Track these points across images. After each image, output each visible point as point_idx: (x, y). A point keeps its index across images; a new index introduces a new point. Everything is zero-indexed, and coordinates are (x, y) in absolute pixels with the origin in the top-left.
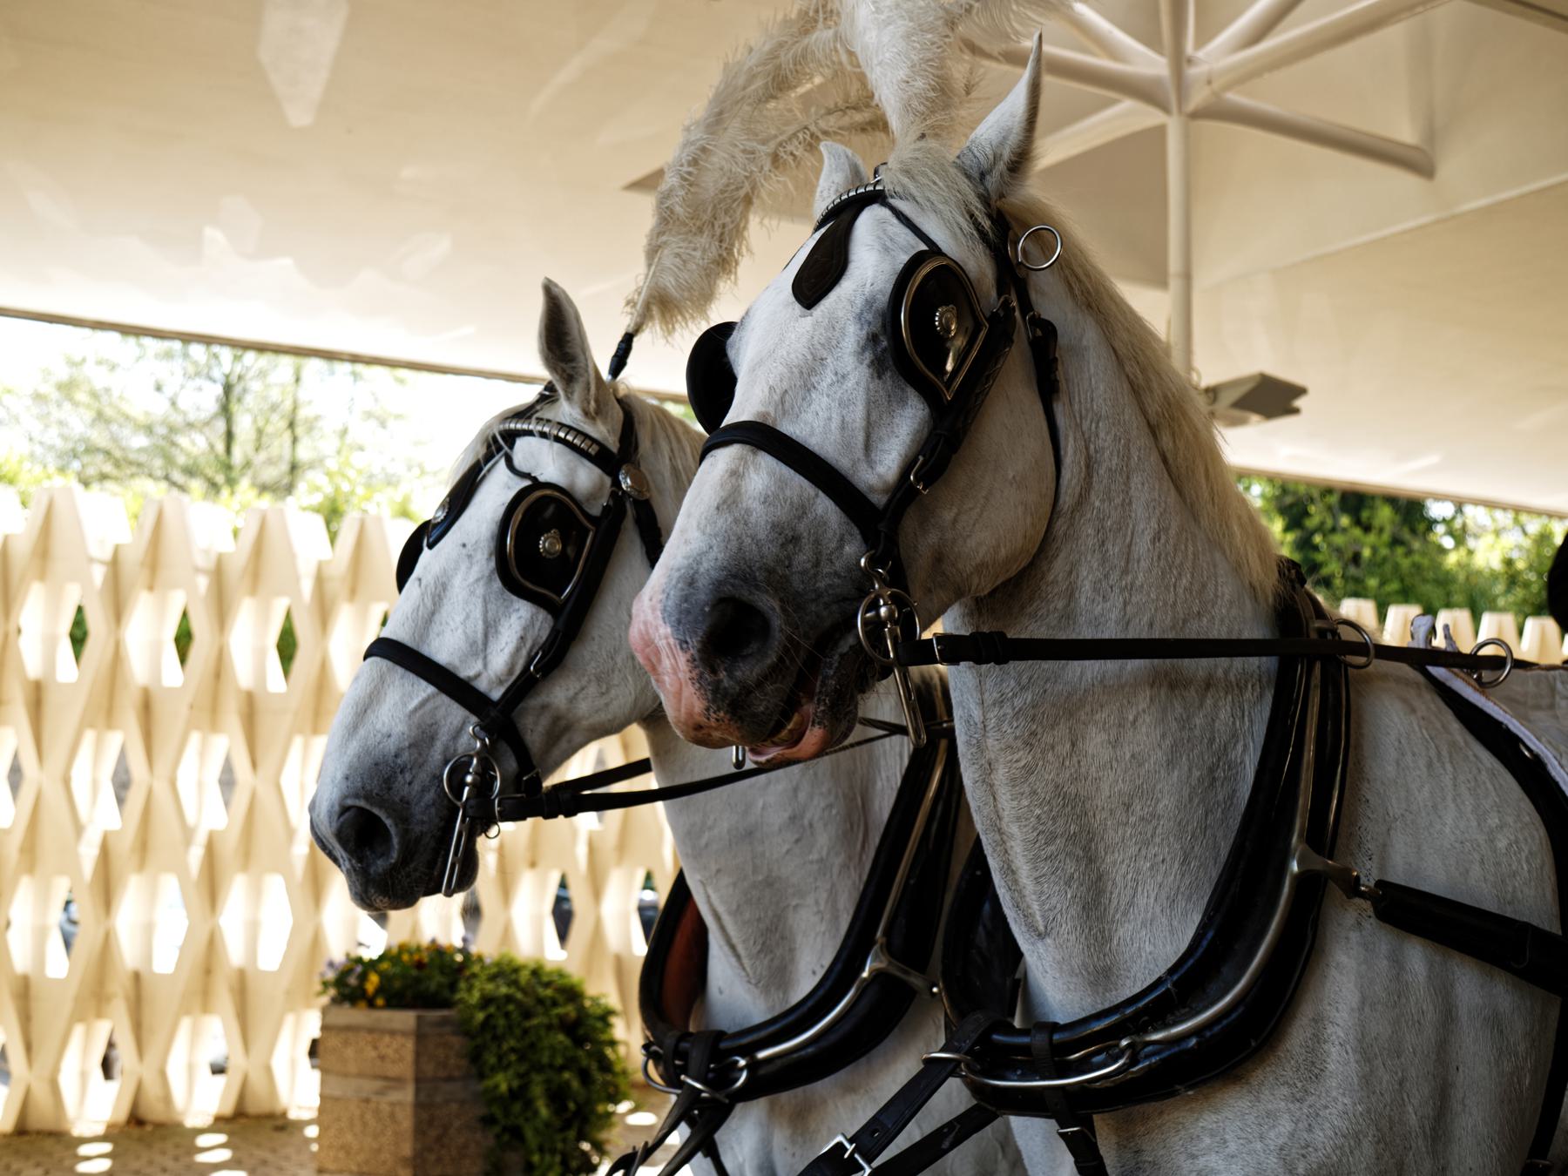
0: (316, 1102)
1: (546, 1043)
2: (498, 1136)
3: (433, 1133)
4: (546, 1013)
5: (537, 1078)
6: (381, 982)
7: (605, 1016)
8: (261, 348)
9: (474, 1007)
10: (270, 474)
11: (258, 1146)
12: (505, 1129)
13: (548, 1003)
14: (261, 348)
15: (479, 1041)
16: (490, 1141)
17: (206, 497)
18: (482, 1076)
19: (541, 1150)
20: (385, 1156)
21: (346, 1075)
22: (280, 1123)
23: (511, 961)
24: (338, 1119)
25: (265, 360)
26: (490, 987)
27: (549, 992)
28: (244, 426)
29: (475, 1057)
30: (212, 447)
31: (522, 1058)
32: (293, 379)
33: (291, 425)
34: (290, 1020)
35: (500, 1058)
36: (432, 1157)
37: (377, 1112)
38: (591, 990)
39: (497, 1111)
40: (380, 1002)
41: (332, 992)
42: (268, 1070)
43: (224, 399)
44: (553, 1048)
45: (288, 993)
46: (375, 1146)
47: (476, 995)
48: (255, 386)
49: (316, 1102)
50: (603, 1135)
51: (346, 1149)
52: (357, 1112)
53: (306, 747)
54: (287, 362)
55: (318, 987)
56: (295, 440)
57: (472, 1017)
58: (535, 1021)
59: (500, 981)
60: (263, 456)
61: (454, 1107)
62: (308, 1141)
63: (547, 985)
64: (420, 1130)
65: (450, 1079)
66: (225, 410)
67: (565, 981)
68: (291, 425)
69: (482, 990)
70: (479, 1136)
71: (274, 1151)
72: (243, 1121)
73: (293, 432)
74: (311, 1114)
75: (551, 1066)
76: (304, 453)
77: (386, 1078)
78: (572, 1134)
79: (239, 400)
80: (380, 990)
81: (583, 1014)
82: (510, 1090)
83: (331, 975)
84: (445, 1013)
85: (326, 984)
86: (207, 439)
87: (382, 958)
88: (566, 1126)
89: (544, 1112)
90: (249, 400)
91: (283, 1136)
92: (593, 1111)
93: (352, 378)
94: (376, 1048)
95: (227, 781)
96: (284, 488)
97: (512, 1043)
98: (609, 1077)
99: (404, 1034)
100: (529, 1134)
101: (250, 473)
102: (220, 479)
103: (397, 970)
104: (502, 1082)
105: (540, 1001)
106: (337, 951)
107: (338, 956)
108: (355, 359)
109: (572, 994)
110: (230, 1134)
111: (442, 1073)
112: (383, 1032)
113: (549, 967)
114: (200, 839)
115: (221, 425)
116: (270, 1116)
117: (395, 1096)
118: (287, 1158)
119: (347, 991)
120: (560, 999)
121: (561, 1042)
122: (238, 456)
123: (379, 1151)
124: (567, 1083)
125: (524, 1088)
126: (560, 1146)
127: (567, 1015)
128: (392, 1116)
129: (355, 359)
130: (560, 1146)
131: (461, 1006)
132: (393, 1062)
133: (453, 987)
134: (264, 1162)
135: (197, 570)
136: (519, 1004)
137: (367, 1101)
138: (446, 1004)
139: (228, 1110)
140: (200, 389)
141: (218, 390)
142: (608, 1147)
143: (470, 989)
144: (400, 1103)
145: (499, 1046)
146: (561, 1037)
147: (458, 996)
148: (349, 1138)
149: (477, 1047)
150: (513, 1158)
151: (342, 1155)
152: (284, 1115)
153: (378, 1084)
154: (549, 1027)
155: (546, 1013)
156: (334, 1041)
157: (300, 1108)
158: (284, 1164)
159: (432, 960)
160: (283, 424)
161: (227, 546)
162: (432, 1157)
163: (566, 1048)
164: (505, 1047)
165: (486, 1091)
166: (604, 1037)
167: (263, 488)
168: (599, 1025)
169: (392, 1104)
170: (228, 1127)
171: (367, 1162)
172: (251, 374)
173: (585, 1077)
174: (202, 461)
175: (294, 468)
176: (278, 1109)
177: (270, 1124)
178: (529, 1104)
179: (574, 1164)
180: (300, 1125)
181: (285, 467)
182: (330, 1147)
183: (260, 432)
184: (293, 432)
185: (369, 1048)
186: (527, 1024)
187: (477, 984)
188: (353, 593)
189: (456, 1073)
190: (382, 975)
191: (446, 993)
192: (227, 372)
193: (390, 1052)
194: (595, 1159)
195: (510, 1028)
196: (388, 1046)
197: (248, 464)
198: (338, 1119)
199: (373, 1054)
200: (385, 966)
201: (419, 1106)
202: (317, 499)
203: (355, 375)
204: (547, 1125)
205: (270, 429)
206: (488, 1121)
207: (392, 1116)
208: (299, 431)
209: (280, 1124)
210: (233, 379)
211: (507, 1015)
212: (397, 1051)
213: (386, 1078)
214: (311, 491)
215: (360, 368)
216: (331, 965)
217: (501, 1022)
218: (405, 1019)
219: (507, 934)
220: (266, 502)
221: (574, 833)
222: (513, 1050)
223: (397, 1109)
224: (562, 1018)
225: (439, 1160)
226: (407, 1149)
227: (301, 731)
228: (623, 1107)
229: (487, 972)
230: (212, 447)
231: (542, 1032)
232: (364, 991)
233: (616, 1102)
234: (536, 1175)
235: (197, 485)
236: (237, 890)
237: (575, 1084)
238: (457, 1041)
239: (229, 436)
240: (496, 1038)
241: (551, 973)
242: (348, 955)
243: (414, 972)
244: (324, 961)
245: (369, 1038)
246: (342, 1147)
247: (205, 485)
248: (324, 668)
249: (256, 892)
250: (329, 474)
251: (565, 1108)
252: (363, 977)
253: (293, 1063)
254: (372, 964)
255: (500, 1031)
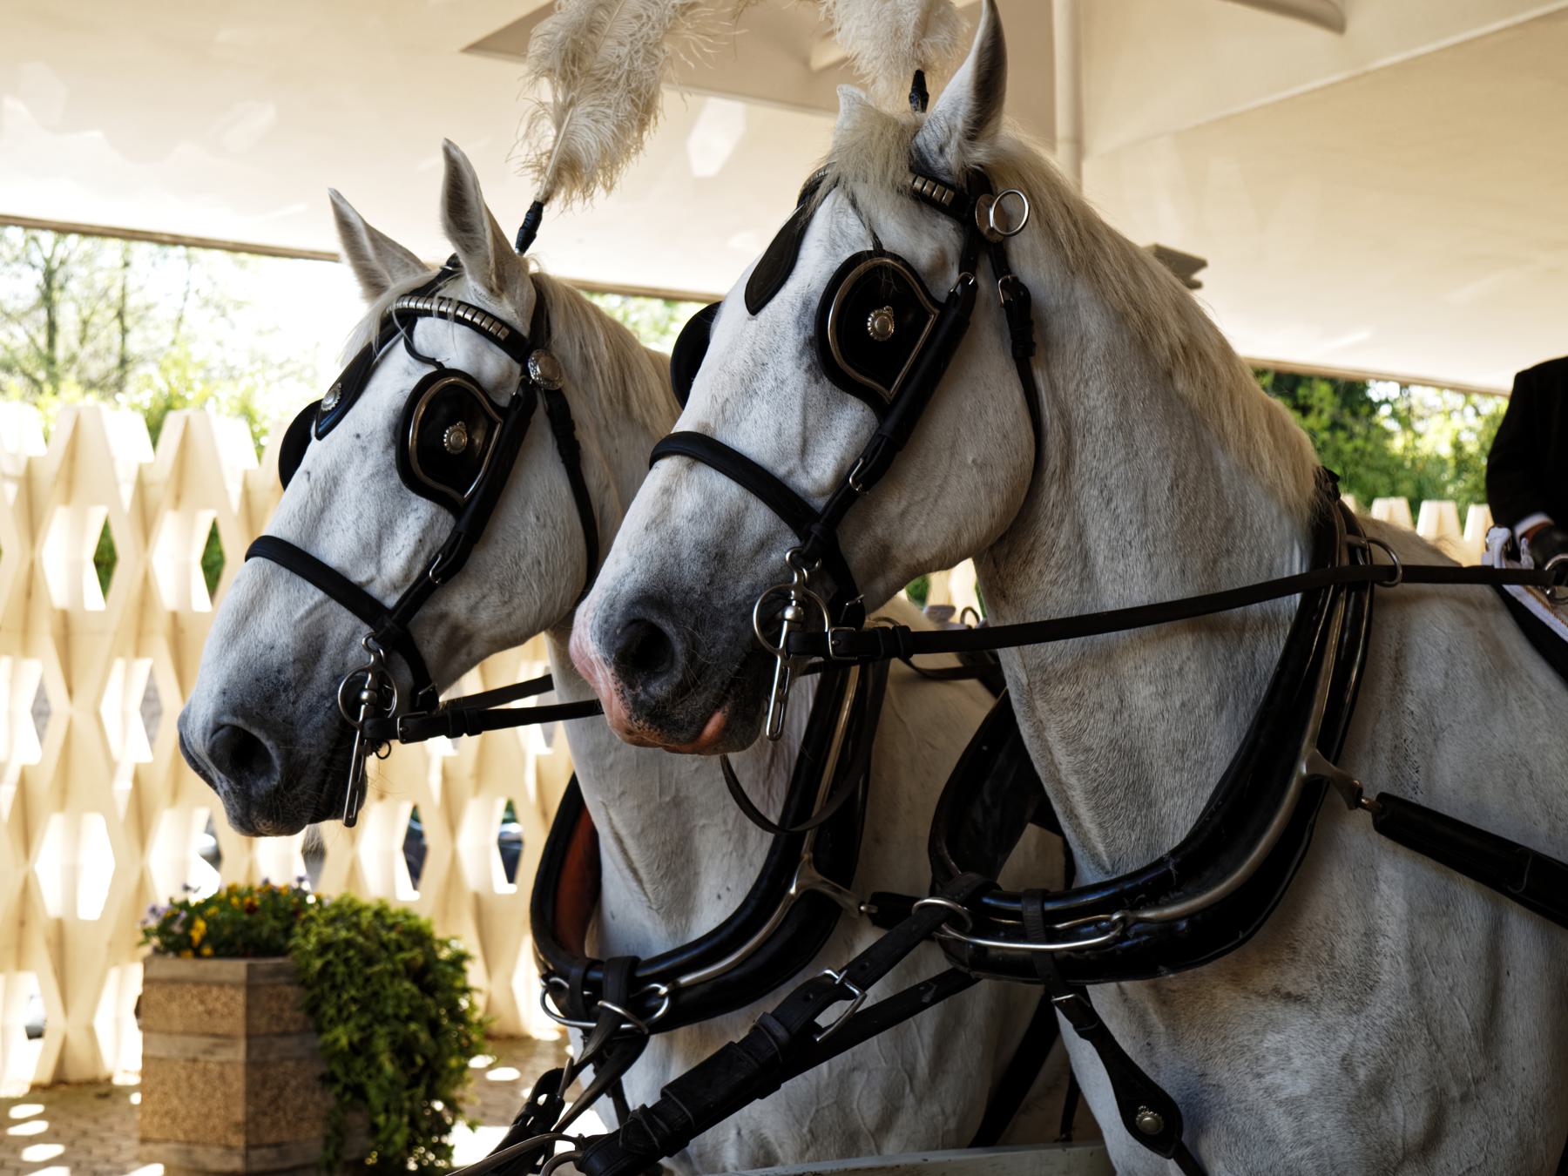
0: (139, 1065)
1: (390, 992)
2: (339, 1097)
3: (267, 1095)
4: (390, 958)
5: (381, 1030)
6: (207, 928)
7: (459, 960)
8: (86, 232)
9: (310, 953)
10: (95, 370)
11: (79, 1116)
12: (346, 1088)
13: (393, 947)
14: (86, 232)
15: (317, 991)
16: (331, 1102)
17: (23, 398)
18: (320, 1031)
19: (387, 1110)
20: (215, 1121)
21: (170, 1033)
22: (103, 1090)
23: (352, 902)
24: (163, 1083)
25: (88, 244)
26: (329, 931)
27: (393, 935)
28: (68, 318)
29: (313, 1009)
30: (33, 340)
31: (364, 1009)
32: (121, 263)
33: (120, 315)
34: (114, 974)
35: (340, 1010)
36: (267, 1121)
37: (205, 1072)
38: (439, 933)
39: (340, 1072)
40: (207, 951)
41: (155, 941)
42: (91, 1031)
43: (45, 287)
44: (398, 997)
45: (110, 944)
46: (205, 1110)
47: (313, 939)
48: (81, 271)
49: (138, 1065)
50: (457, 1093)
51: (171, 1114)
52: (183, 1074)
53: (128, 671)
54: (114, 245)
55: (141, 937)
56: (125, 331)
57: (308, 965)
58: (377, 968)
59: (339, 925)
60: (89, 348)
61: (290, 1065)
62: (132, 1108)
63: (392, 927)
64: (252, 1093)
65: (285, 1034)
66: (47, 299)
67: (412, 922)
68: (120, 315)
69: (319, 934)
70: (317, 1097)
71: (96, 1121)
72: (63, 1088)
73: (122, 322)
74: (135, 1080)
75: (396, 1016)
76: (135, 345)
77: (215, 1035)
78: (421, 1091)
79: (62, 288)
80: (206, 938)
81: (431, 961)
82: (351, 1044)
83: (153, 923)
84: (280, 960)
85: (147, 933)
86: (27, 332)
87: (209, 902)
88: (414, 1082)
89: (389, 1068)
90: (73, 286)
91: (106, 1104)
92: (444, 1066)
93: (185, 262)
94: (202, 1002)
95: (41, 713)
96: (113, 383)
97: (353, 992)
98: (461, 1028)
99: (234, 985)
100: (372, 1092)
101: (75, 368)
102: (41, 375)
103: (226, 915)
104: (342, 1036)
105: (384, 945)
106: (164, 893)
107: (163, 903)
108: (176, 241)
109: (420, 937)
110: (47, 1103)
111: (276, 1029)
112: (211, 984)
113: (393, 909)
114: (12, 775)
115: (42, 315)
116: (93, 1083)
117: (225, 1055)
118: (111, 1129)
119: (170, 940)
120: (406, 943)
121: (406, 990)
122: (60, 353)
123: (208, 1116)
124: (415, 1035)
125: (367, 1041)
126: (407, 1105)
127: (413, 959)
128: (222, 1076)
129: (176, 241)
130: (407, 1105)
131: (296, 953)
132: (223, 1016)
133: (287, 932)
134: (85, 1134)
135: (5, 477)
136: (360, 949)
137: (195, 1060)
138: (281, 952)
139: (46, 1077)
140: (19, 276)
141: (38, 276)
142: (463, 1106)
143: (305, 935)
144: (229, 1062)
145: (339, 996)
146: (407, 985)
147: (292, 942)
148: (175, 1102)
149: (313, 998)
150: (357, 1120)
151: (167, 1121)
152: (109, 1080)
153: (206, 1042)
154: (394, 974)
155: (390, 958)
156: (157, 995)
157: (126, 1072)
158: (106, 1135)
159: (264, 903)
160: (113, 313)
161: (37, 449)
162: (267, 1121)
163: (413, 997)
164: (345, 996)
165: (324, 1047)
166: (459, 984)
167: (90, 385)
168: (450, 970)
169: (222, 1064)
170: (44, 1096)
171: (195, 1129)
172: (73, 258)
173: (434, 1027)
174: (21, 355)
175: (123, 362)
176: (102, 1075)
177: (93, 1091)
178: (372, 1059)
179: (424, 1125)
180: (125, 1091)
181: (113, 361)
182: (155, 1113)
183: (85, 323)
184: (122, 322)
185: (195, 1002)
186: (369, 971)
187: (314, 928)
188: (178, 498)
189: (292, 1028)
190: (207, 920)
191: (282, 941)
192: (48, 255)
193: (218, 1006)
194: (449, 1120)
195: (350, 975)
196: (217, 999)
197: (72, 359)
198: (163, 1083)
199: (201, 1008)
200: (212, 910)
201: (251, 1064)
202: (147, 399)
203: (188, 257)
204: (393, 1082)
205: (96, 319)
206: (328, 1079)
207: (222, 1076)
208: (129, 321)
209: (103, 1091)
210: (55, 264)
211: (347, 961)
212: (225, 1005)
213: (215, 1035)
214: (143, 390)
215: (195, 251)
216: (153, 910)
217: (341, 969)
218: (236, 969)
219: (354, 872)
220: (93, 396)
221: (427, 760)
222: (354, 1000)
223: (228, 1069)
224: (406, 963)
225: (274, 1124)
226: (239, 1114)
227: (121, 655)
228: (477, 1062)
229: (324, 914)
230: (33, 340)
231: (386, 980)
232: (190, 939)
233: (471, 1055)
234: (382, 1136)
235: (16, 383)
236: (53, 833)
237: (424, 1036)
238: (292, 992)
239: (52, 327)
240: (333, 987)
241: (395, 916)
242: (171, 900)
243: (245, 917)
244: (149, 906)
245: (195, 991)
246: (167, 1113)
247: (26, 381)
248: (147, 581)
249: (75, 834)
250: (162, 369)
251: (413, 1063)
252: (189, 924)
253: (118, 1022)
254: (201, 908)
255: (339, 979)
